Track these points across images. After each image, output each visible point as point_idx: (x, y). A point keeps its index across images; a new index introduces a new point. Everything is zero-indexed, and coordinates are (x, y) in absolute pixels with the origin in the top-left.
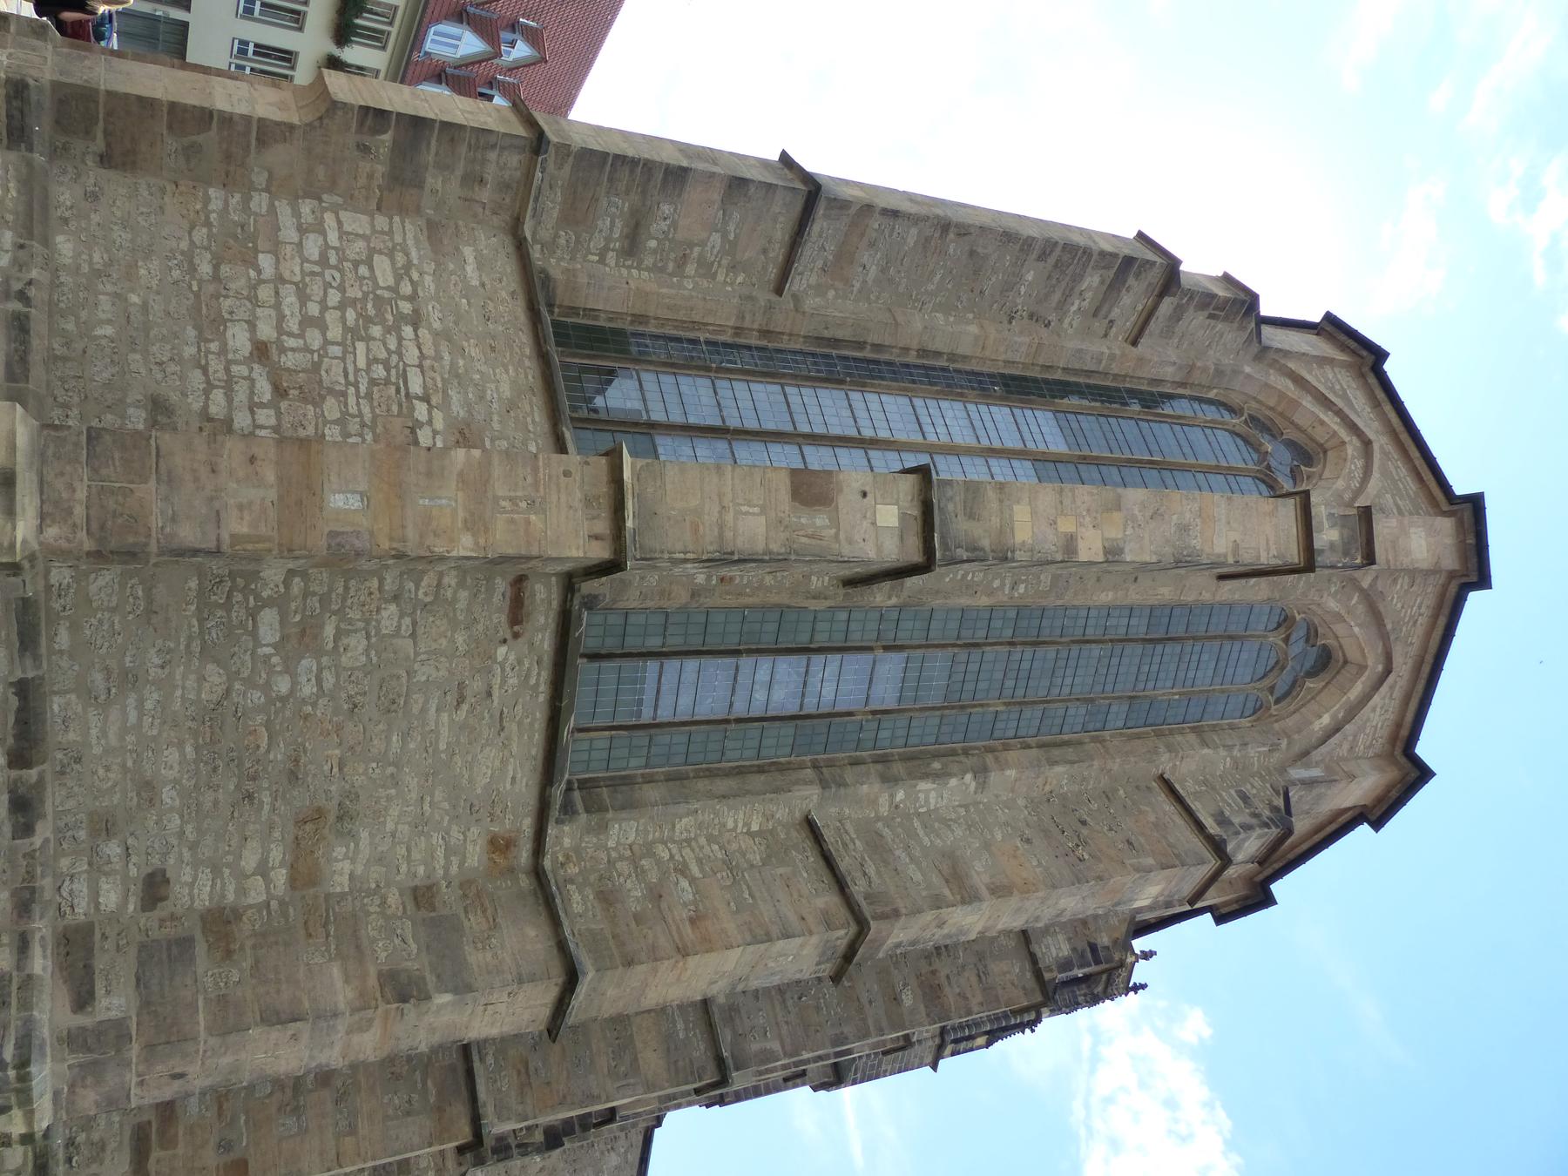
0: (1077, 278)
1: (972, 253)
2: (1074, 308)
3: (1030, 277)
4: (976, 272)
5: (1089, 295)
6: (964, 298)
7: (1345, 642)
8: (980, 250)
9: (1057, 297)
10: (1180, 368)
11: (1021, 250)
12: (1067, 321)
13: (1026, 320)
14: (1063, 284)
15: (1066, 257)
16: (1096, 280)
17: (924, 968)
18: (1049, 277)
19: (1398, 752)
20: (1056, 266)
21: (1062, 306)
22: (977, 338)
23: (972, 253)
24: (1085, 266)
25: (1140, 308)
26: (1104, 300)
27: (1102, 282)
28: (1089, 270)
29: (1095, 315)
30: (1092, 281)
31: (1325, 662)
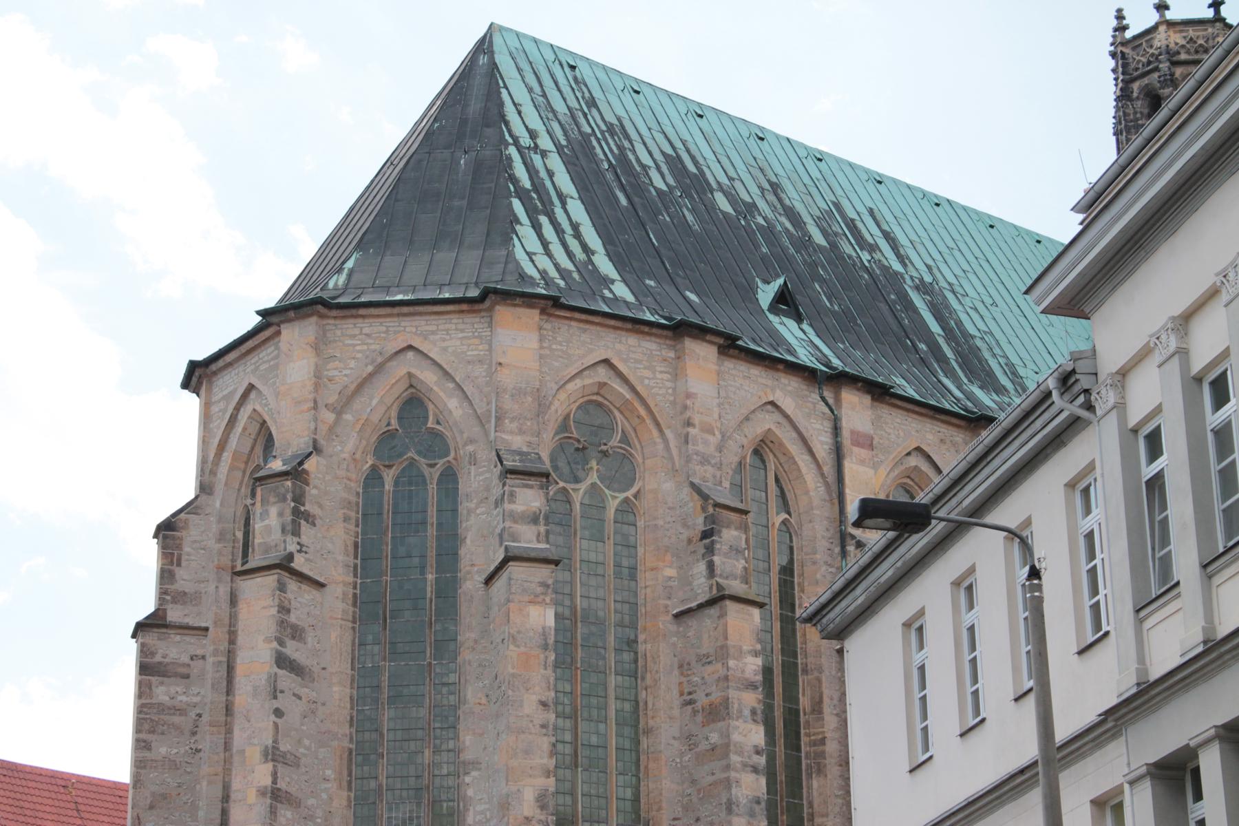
0: (162, 708)
1: (151, 807)
2: (184, 698)
3: (163, 750)
4: (164, 797)
5: (173, 690)
6: (184, 799)
7: (389, 401)
8: (149, 802)
9: (176, 719)
10: (220, 580)
11: (145, 767)
12: (196, 699)
13: (198, 737)
14: (166, 718)
15: (146, 726)
16: (162, 689)
17: (699, 718)
18: (163, 734)
19: (481, 306)
20: (153, 732)
21: (182, 712)
22: (210, 783)
23: (151, 807)
24: (151, 706)
25: (178, 638)
26: (176, 675)
27: (162, 683)
28: (154, 701)
29: (187, 677)
30: (162, 692)
31: (413, 404)
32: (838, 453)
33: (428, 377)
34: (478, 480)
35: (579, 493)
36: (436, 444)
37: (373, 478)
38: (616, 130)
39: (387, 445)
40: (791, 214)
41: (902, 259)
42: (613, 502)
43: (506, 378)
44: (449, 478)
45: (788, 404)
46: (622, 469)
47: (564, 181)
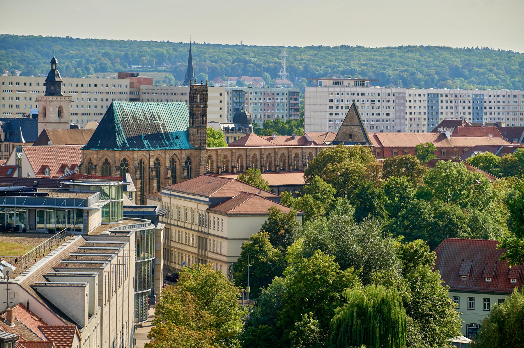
31: (106, 160)
32: (150, 158)
33: (108, 158)
34: (113, 168)
35: (123, 168)
36: (109, 164)
37: (102, 167)
38: (126, 115)
39: (104, 164)
40: (146, 119)
41: (160, 119)
42: (126, 168)
43: (116, 159)
44: (110, 167)
45: (144, 154)
46: (127, 165)
47: (122, 129)
